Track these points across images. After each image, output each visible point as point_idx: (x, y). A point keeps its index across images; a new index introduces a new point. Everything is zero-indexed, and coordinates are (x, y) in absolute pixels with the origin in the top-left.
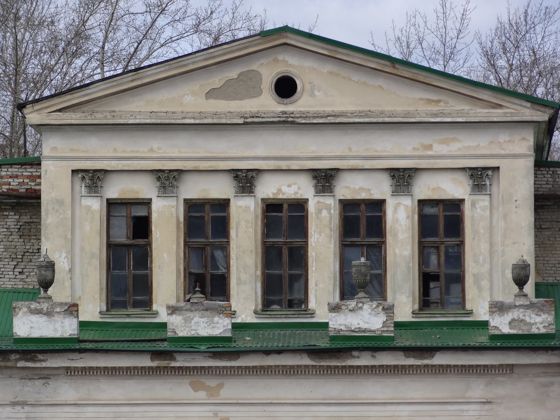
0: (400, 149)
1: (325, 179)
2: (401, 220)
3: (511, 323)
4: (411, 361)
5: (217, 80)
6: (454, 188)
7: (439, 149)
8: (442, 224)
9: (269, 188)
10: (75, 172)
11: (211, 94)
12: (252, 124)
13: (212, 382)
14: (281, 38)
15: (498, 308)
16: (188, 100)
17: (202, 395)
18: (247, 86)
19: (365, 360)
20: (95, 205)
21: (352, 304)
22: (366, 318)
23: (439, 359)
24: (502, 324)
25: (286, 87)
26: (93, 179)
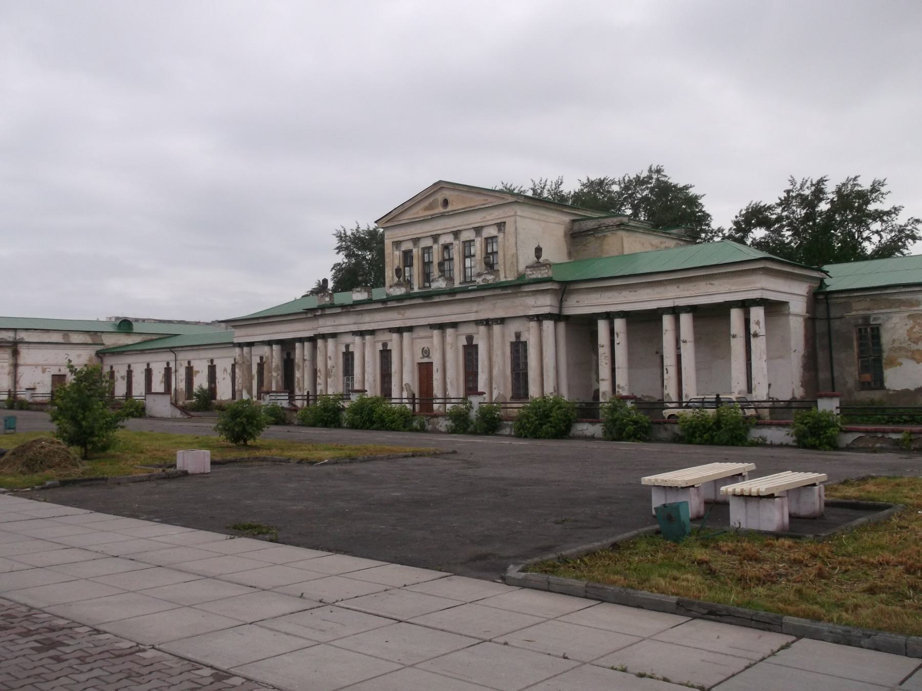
0: (476, 219)
1: (456, 234)
3: (484, 280)
4: (450, 298)
5: (426, 203)
6: (493, 231)
7: (489, 218)
11: (427, 209)
12: (433, 218)
13: (402, 312)
14: (440, 186)
15: (479, 275)
16: (418, 212)
17: (400, 316)
19: (437, 299)
22: (441, 284)
23: (458, 297)
24: (479, 281)
25: (446, 203)
26: (397, 244)
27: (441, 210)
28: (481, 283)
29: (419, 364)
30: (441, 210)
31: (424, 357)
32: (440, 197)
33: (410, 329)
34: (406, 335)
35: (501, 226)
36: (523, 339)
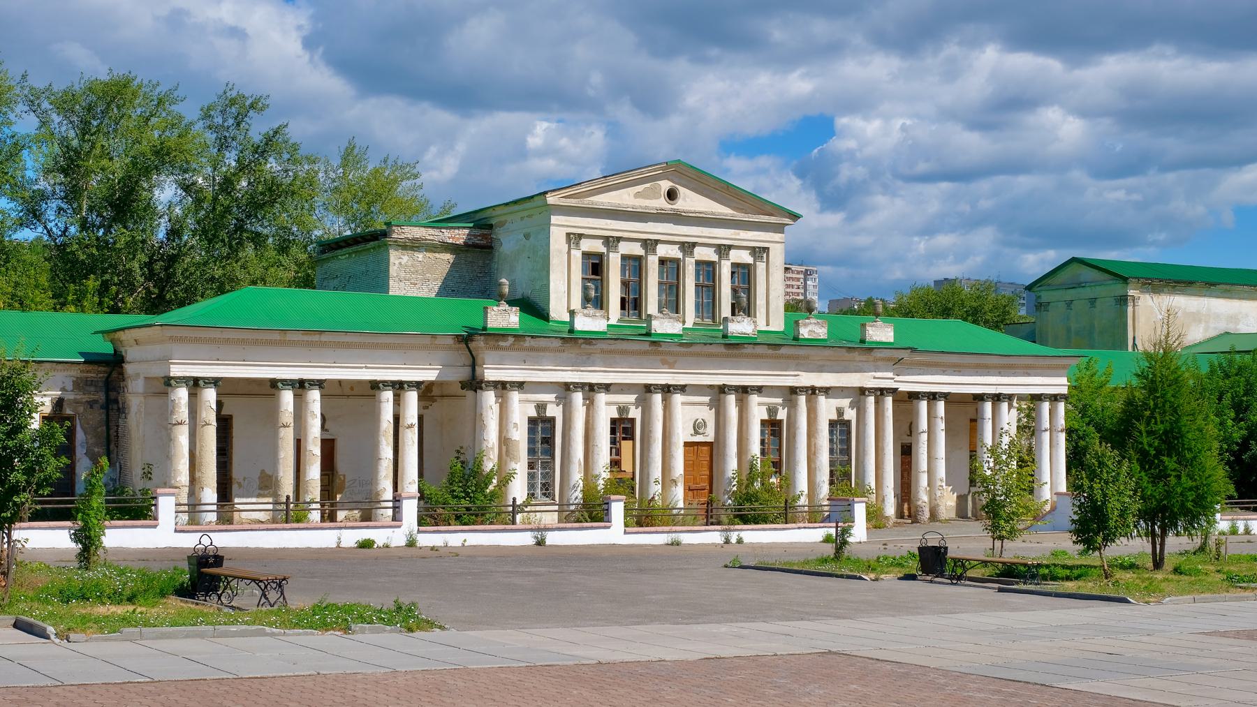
2: (725, 270)
4: (770, 352)
5: (640, 188)
6: (745, 257)
8: (744, 274)
9: (663, 251)
10: (568, 235)
11: (637, 195)
16: (625, 198)
18: (654, 194)
19: (749, 350)
20: (577, 255)
21: (739, 318)
25: (672, 195)
26: (574, 239)
27: (662, 203)
28: (806, 336)
29: (687, 444)
30: (662, 203)
31: (696, 433)
32: (665, 185)
33: (682, 389)
34: (678, 398)
35: (760, 252)
36: (846, 417)
